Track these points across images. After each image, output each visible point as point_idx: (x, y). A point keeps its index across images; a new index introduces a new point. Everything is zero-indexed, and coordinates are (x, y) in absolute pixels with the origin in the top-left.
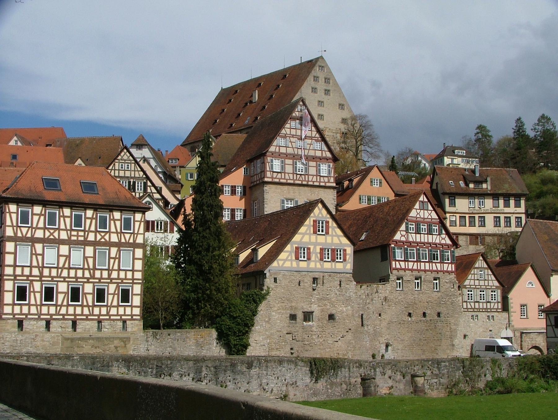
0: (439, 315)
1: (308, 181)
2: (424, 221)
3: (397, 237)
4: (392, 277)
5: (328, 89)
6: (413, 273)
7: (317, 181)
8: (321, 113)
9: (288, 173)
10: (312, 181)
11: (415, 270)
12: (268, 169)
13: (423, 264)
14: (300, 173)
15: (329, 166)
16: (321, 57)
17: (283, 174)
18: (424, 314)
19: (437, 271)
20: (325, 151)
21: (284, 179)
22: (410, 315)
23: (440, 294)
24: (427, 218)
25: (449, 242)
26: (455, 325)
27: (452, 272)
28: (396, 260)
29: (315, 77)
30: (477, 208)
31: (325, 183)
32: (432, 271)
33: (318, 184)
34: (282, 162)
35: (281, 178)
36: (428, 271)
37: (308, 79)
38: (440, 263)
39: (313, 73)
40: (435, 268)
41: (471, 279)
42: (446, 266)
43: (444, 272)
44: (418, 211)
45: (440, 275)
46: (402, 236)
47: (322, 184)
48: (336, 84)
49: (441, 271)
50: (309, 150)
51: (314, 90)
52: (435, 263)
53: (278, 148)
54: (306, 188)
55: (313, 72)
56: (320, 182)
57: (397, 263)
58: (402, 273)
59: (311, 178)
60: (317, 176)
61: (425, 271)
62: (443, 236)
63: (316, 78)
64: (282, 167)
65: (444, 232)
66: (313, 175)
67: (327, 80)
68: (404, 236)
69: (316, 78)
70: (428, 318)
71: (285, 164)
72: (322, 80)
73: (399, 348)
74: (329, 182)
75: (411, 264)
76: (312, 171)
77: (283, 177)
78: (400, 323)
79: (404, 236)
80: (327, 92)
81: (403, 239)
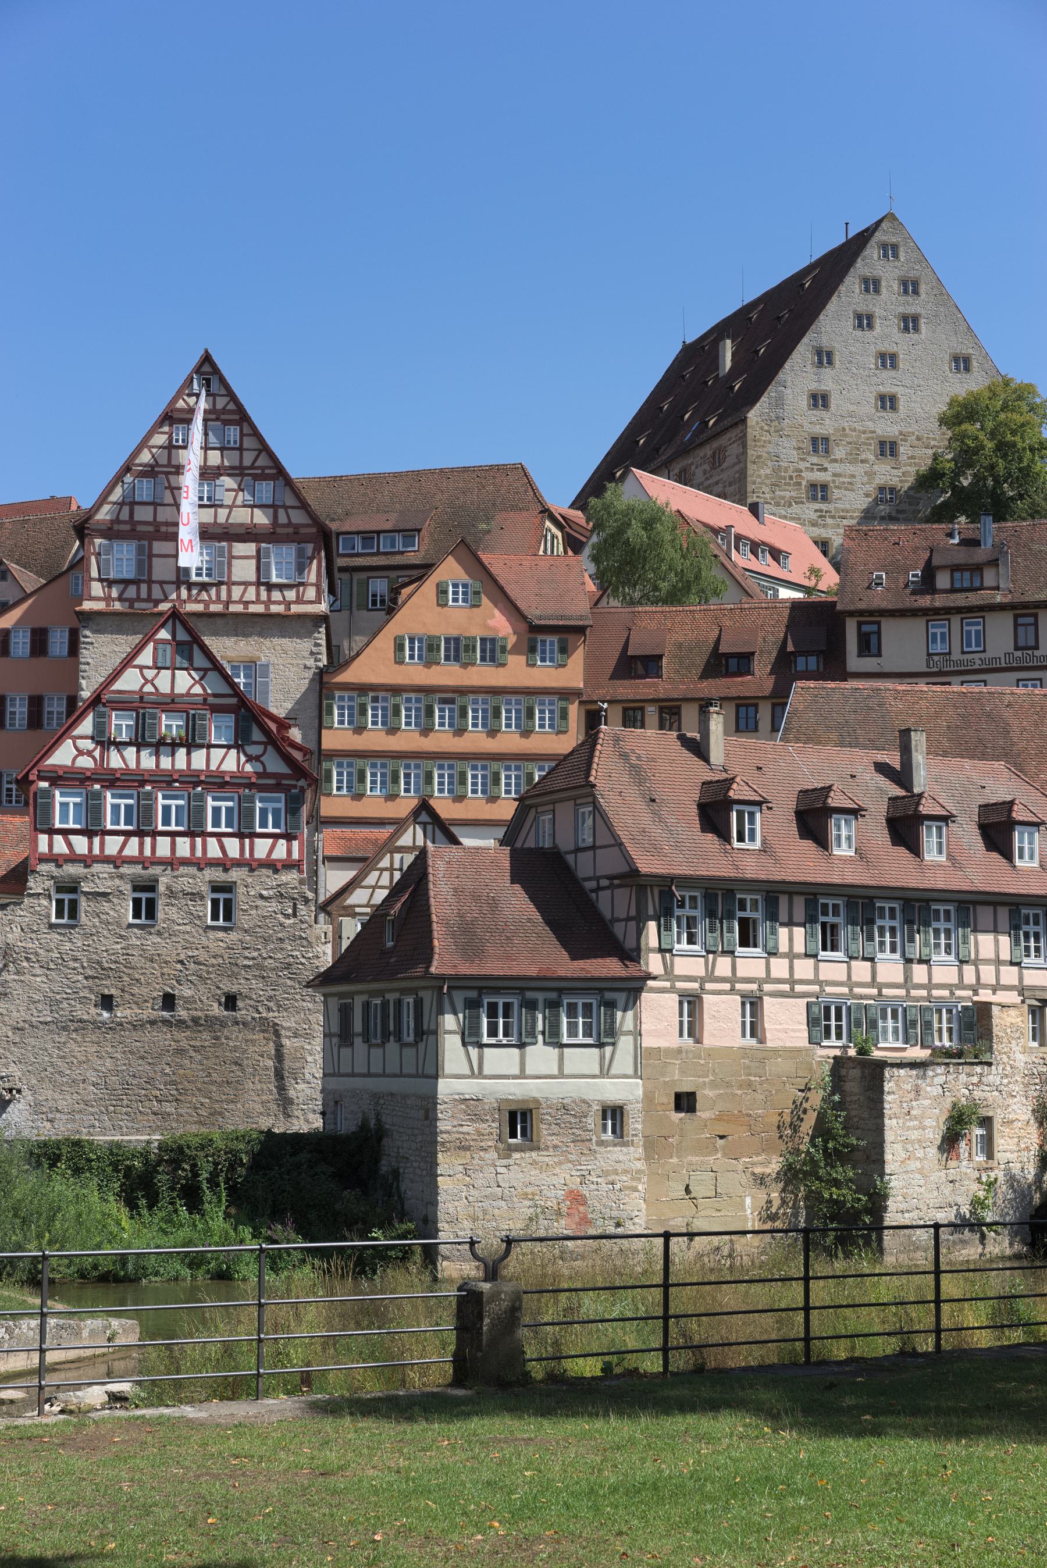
0: (231, 1002)
1: (227, 603)
2: (171, 703)
3: (63, 756)
4: (34, 885)
5: (911, 310)
6: (122, 870)
7: (258, 601)
8: (887, 389)
9: (161, 583)
10: (240, 602)
11: (131, 861)
12: (94, 573)
13: (164, 842)
14: (205, 579)
15: (300, 554)
16: (890, 217)
17: (144, 587)
18: (169, 1001)
19: (224, 864)
20: (286, 508)
21: (149, 599)
22: (107, 1002)
23: (234, 936)
24: (188, 694)
25: (275, 765)
26: (296, 1035)
27: (289, 865)
28: (52, 832)
29: (866, 281)
30: (956, 655)
31: (288, 604)
32: (201, 864)
33: (259, 609)
34: (140, 550)
35: (139, 599)
36: (185, 862)
37: (842, 288)
38: (240, 835)
39: (861, 267)
40: (214, 851)
41: (374, 888)
42: (262, 848)
43: (252, 865)
44: (150, 674)
45: (235, 875)
46: (81, 753)
47: (275, 609)
48: (941, 294)
49: (238, 863)
50: (231, 507)
51: (864, 321)
52: (219, 836)
53: (126, 509)
54: (219, 621)
55: (859, 262)
56: (269, 602)
57: (58, 839)
58: (73, 870)
59: (237, 592)
60: (258, 584)
61: (172, 863)
62: (254, 750)
63: (871, 285)
64: (140, 564)
65: (257, 735)
66: (246, 584)
67: (910, 286)
68: (89, 753)
69: (871, 285)
70: (182, 1013)
71: (151, 556)
72: (890, 286)
73: (62, 1104)
74: (299, 601)
75: (113, 845)
76: (244, 570)
77: (144, 594)
78: (64, 1028)
79: (89, 753)
80: (910, 323)
81: (86, 762)
